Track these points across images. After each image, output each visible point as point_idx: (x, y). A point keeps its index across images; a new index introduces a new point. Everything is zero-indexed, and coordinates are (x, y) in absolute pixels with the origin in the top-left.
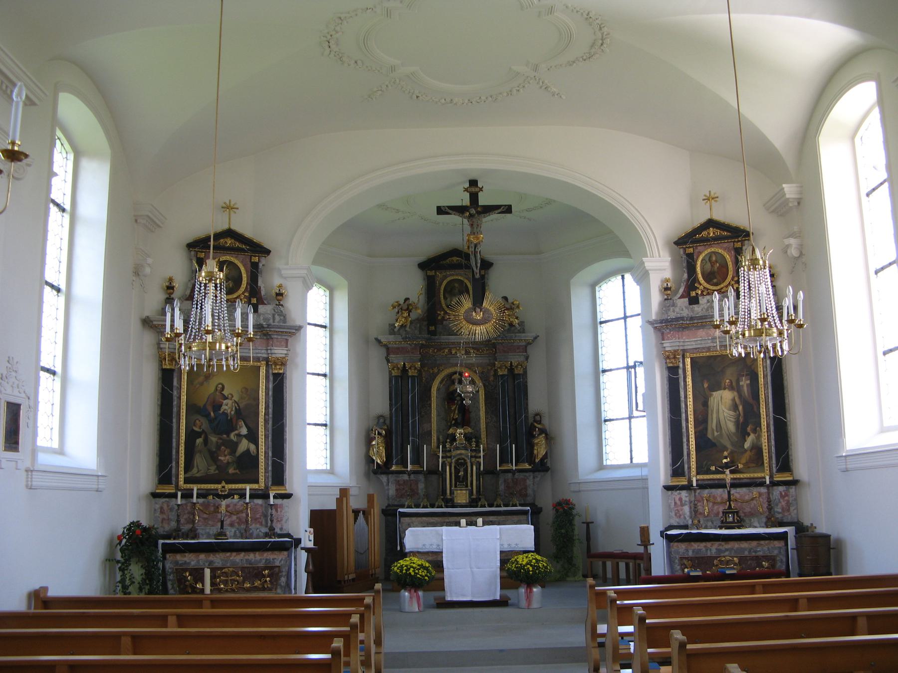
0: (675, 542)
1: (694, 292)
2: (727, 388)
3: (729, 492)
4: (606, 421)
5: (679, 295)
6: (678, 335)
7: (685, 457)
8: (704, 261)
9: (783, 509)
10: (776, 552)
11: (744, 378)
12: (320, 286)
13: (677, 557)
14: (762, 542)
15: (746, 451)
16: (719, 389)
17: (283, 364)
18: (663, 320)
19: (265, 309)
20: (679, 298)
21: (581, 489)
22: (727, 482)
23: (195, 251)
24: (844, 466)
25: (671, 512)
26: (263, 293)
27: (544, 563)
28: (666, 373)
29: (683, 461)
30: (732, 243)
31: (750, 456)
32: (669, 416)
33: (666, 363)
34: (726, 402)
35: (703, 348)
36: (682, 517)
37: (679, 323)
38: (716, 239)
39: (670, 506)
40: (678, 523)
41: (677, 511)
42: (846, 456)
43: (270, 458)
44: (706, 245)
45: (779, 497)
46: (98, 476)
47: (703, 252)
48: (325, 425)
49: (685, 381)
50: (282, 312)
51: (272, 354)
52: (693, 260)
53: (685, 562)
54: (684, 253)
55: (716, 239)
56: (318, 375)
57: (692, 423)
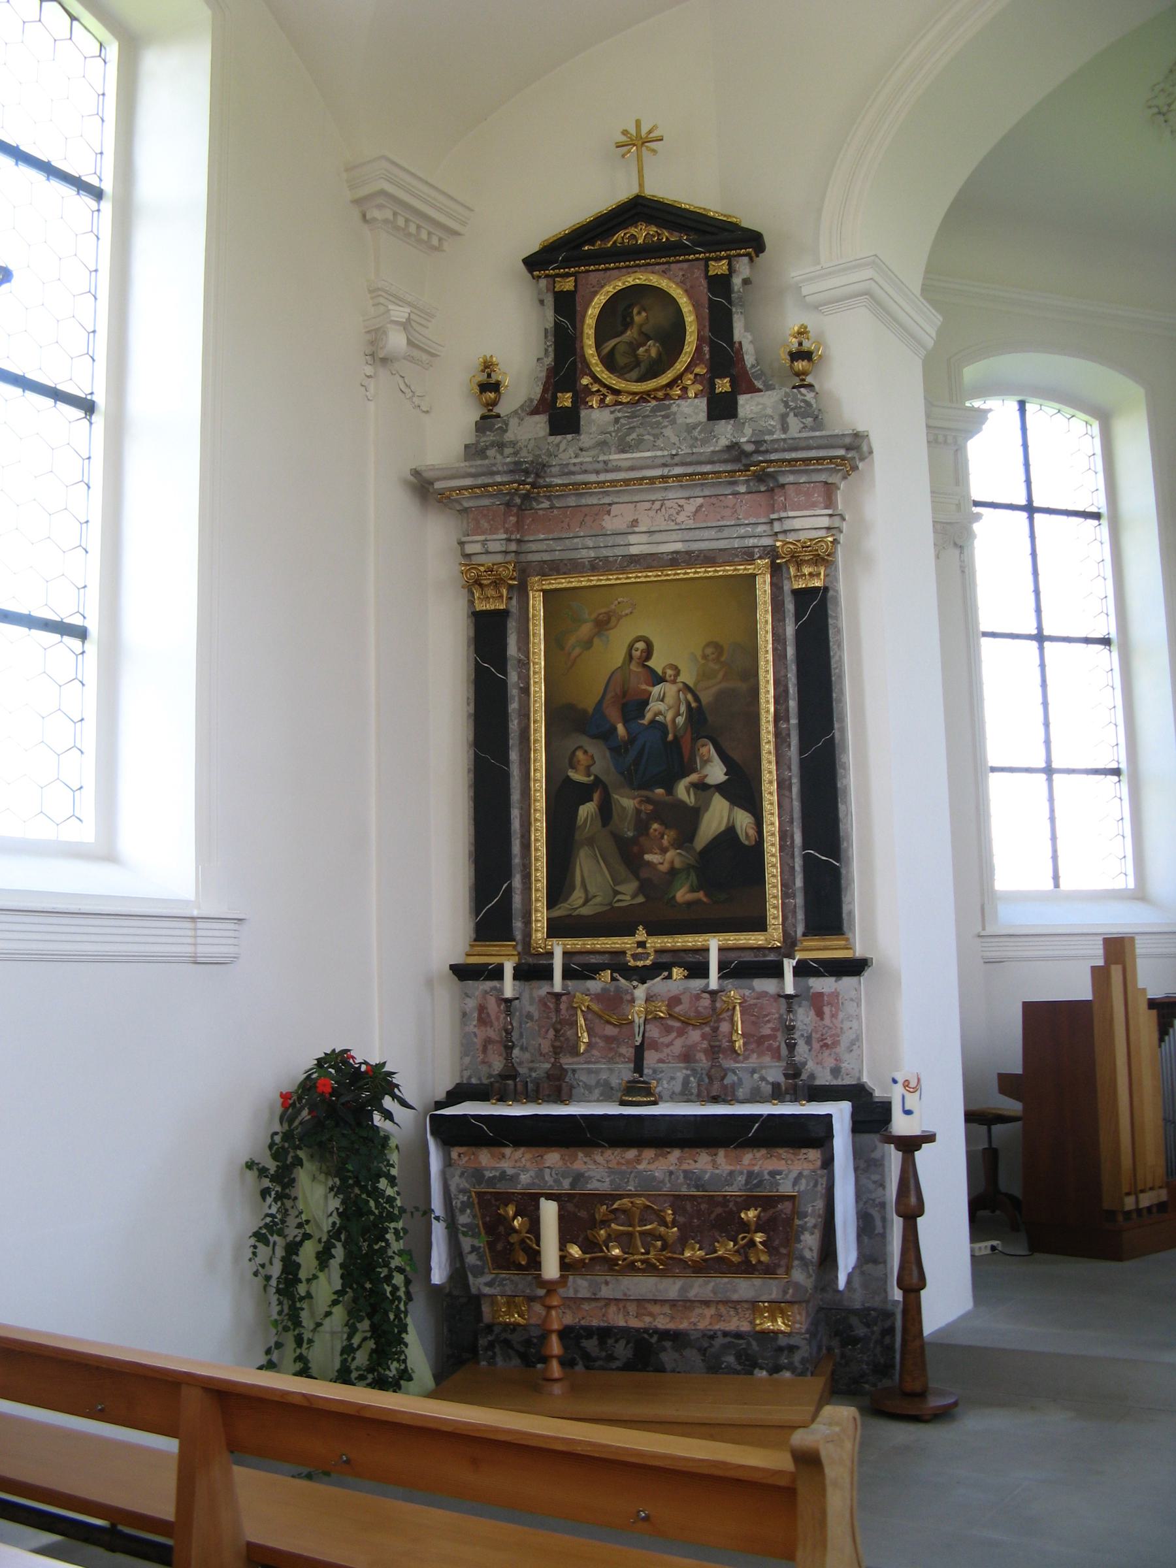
12: (1072, 411)
17: (823, 559)
19: (758, 404)
23: (547, 276)
26: (749, 359)
43: (797, 852)
46: (193, 919)
48: (1116, 772)
50: (808, 404)
51: (785, 532)
56: (1087, 641)
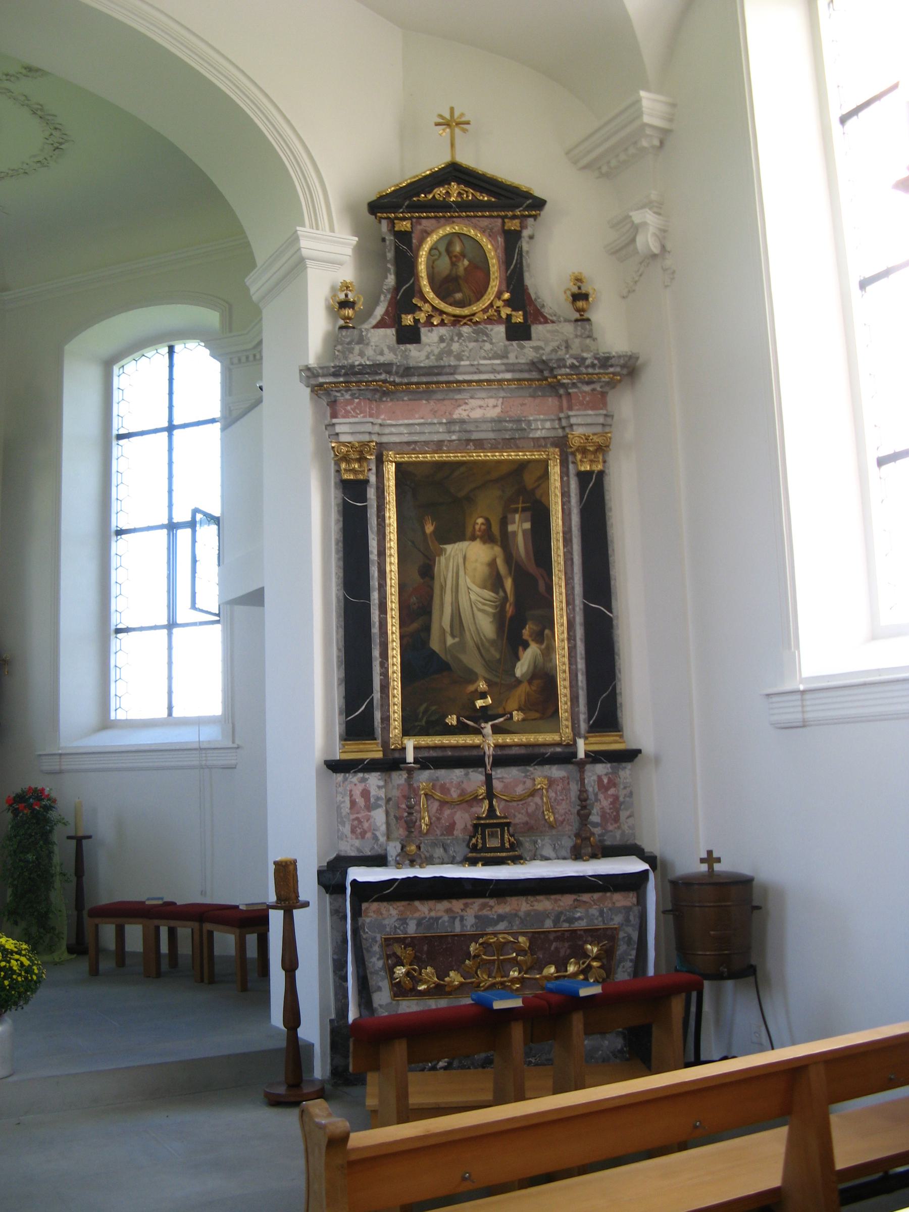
0: (375, 901)
1: (410, 317)
2: (478, 537)
3: (489, 779)
4: (118, 631)
5: (374, 321)
6: (371, 408)
7: (377, 695)
8: (434, 252)
9: (603, 816)
10: (618, 920)
11: (517, 516)
13: (378, 939)
14: (585, 897)
15: (519, 682)
16: (461, 537)
18: (343, 367)
20: (377, 326)
21: (63, 767)
22: (487, 753)
24: (799, 716)
25: (343, 824)
27: (23, 959)
28: (335, 496)
29: (371, 702)
30: (500, 221)
31: (528, 694)
32: (342, 598)
33: (338, 471)
34: (475, 569)
35: (426, 443)
36: (369, 835)
37: (377, 378)
38: (464, 206)
39: (339, 808)
40: (358, 850)
41: (356, 822)
42: (803, 692)
44: (441, 217)
45: (596, 789)
47: (432, 231)
49: (381, 517)
52: (410, 247)
53: (398, 950)
54: (389, 231)
55: (464, 206)
57: (396, 613)
